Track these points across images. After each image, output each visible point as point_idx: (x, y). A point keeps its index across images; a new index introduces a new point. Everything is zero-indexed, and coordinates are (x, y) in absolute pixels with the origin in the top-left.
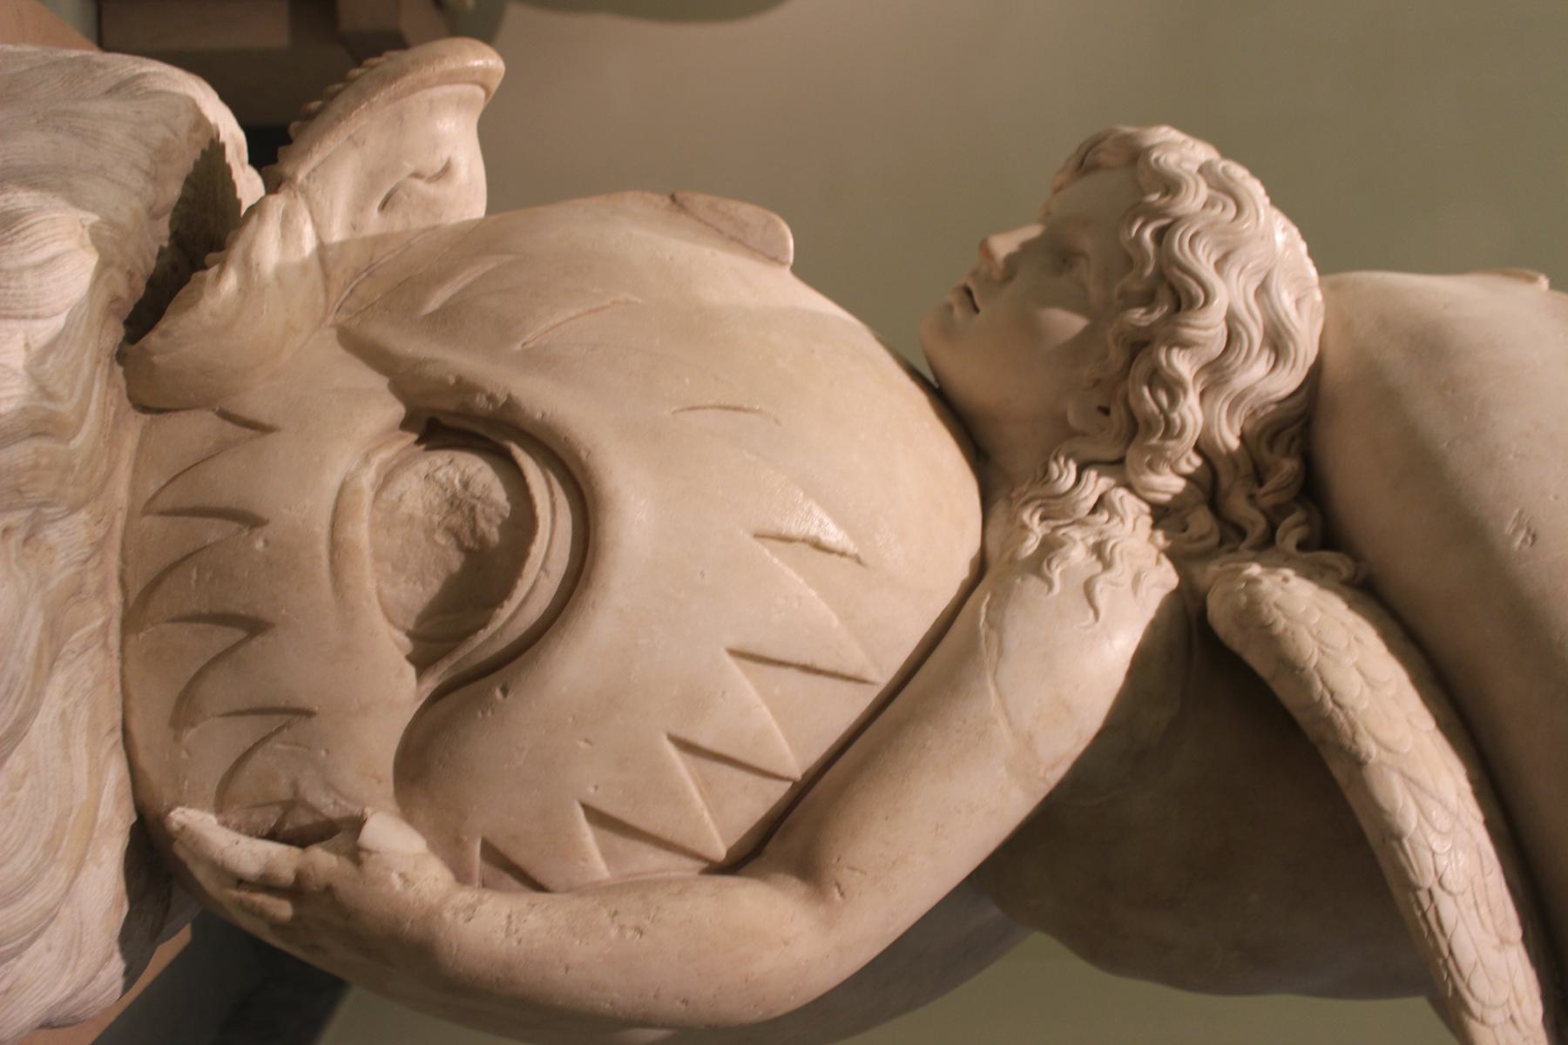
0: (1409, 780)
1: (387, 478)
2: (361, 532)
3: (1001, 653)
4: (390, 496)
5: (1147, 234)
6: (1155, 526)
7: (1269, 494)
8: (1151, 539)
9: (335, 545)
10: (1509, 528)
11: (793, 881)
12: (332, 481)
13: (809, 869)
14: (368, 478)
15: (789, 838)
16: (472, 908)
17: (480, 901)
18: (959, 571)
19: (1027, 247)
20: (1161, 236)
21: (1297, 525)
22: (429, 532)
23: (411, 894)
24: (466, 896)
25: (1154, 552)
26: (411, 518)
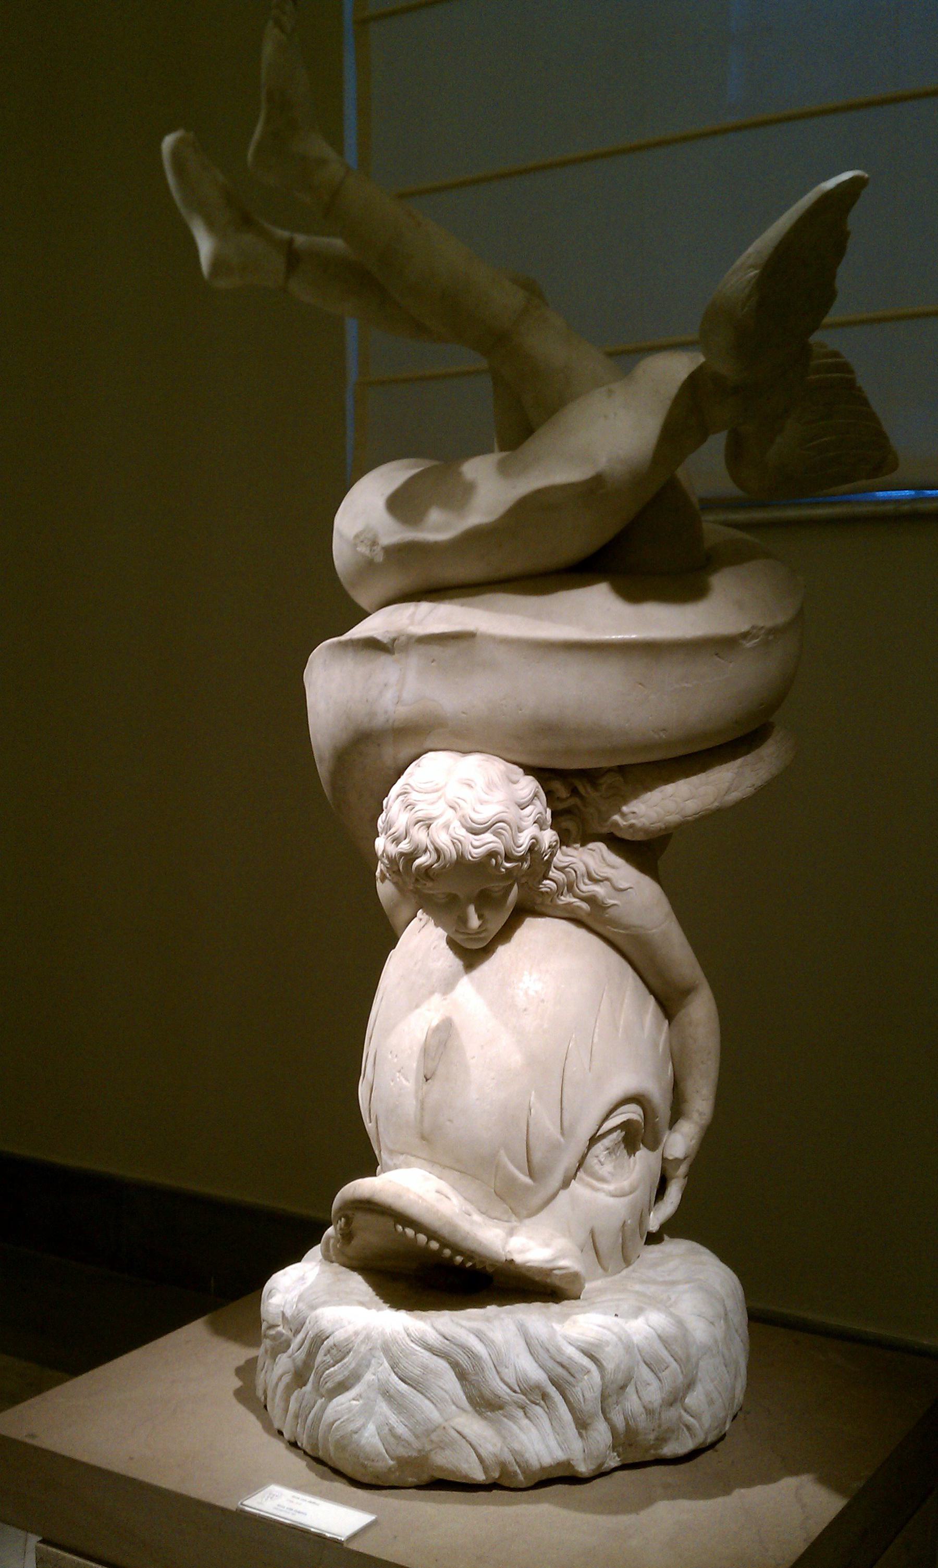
0: (728, 791)
1: (602, 1180)
2: (625, 1184)
3: (641, 927)
4: (609, 1177)
5: (508, 865)
6: (567, 846)
7: (563, 792)
8: (576, 849)
9: (631, 1193)
10: (656, 736)
11: (689, 997)
12: (612, 1200)
13: (686, 992)
14: (611, 1187)
15: (668, 1000)
16: (700, 1114)
17: (698, 1111)
18: (582, 933)
19: (477, 910)
20: (508, 858)
21: (584, 787)
22: (617, 1158)
23: (696, 1137)
24: (695, 1116)
25: (581, 849)
26: (614, 1167)
